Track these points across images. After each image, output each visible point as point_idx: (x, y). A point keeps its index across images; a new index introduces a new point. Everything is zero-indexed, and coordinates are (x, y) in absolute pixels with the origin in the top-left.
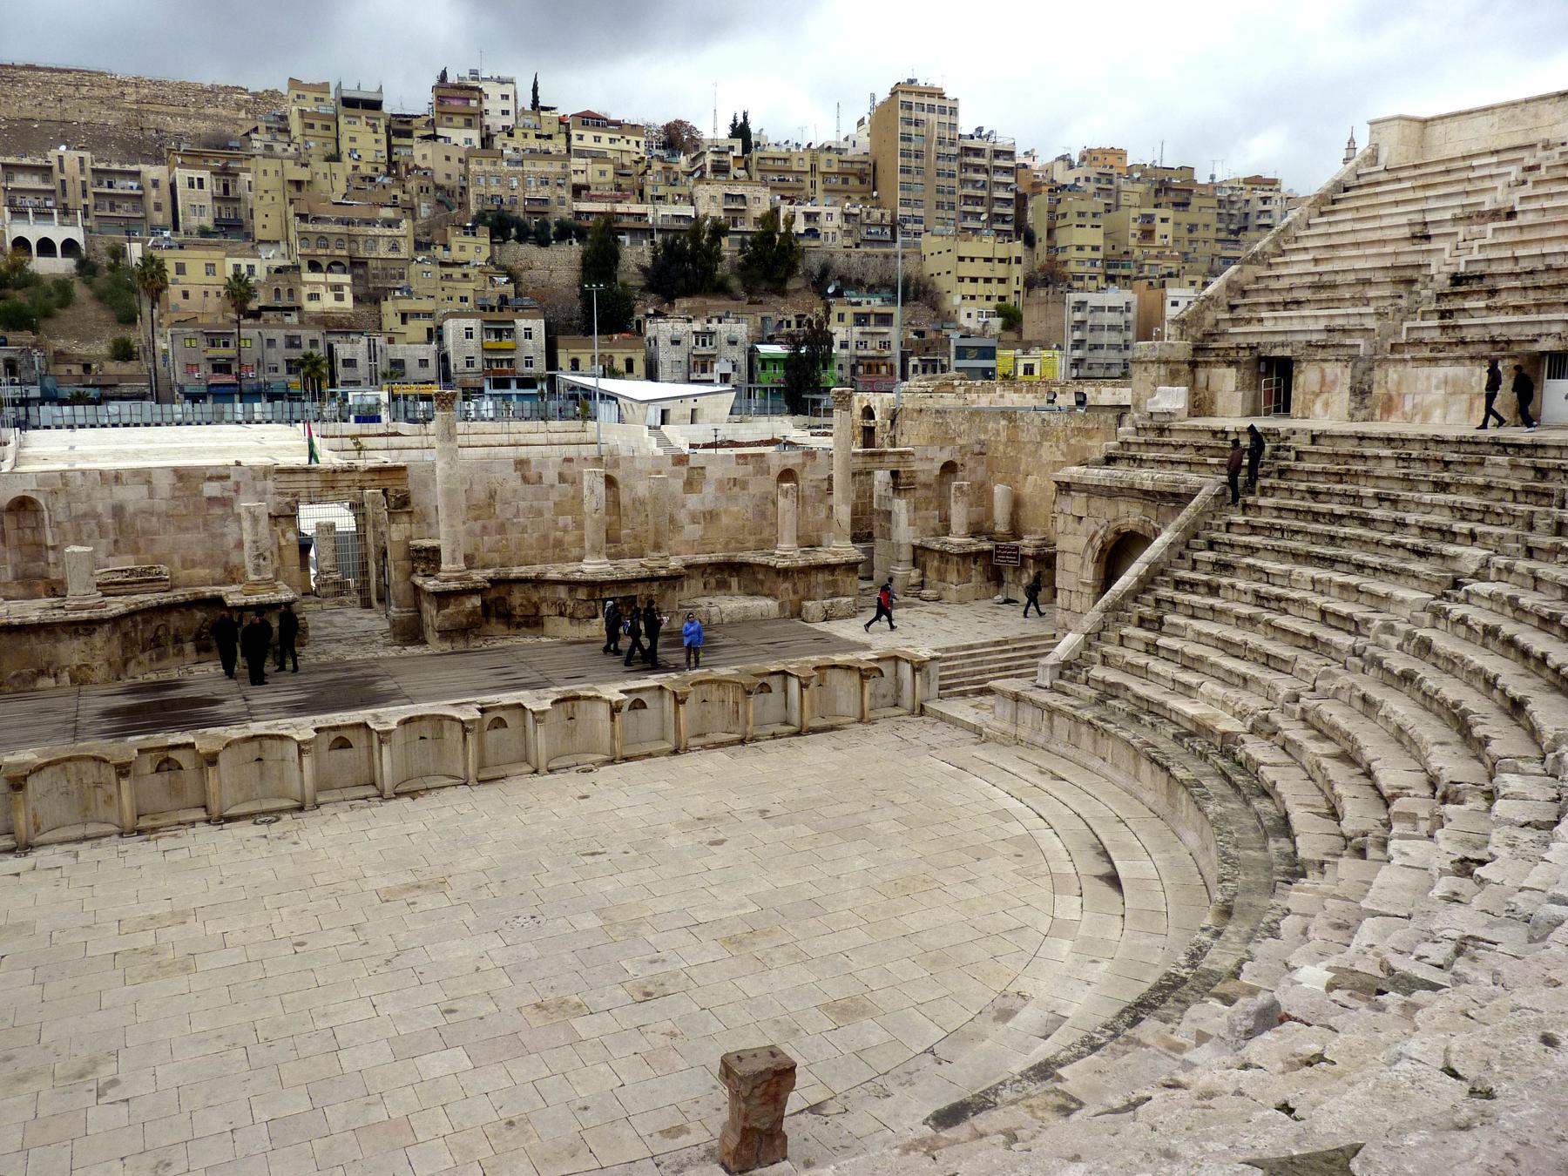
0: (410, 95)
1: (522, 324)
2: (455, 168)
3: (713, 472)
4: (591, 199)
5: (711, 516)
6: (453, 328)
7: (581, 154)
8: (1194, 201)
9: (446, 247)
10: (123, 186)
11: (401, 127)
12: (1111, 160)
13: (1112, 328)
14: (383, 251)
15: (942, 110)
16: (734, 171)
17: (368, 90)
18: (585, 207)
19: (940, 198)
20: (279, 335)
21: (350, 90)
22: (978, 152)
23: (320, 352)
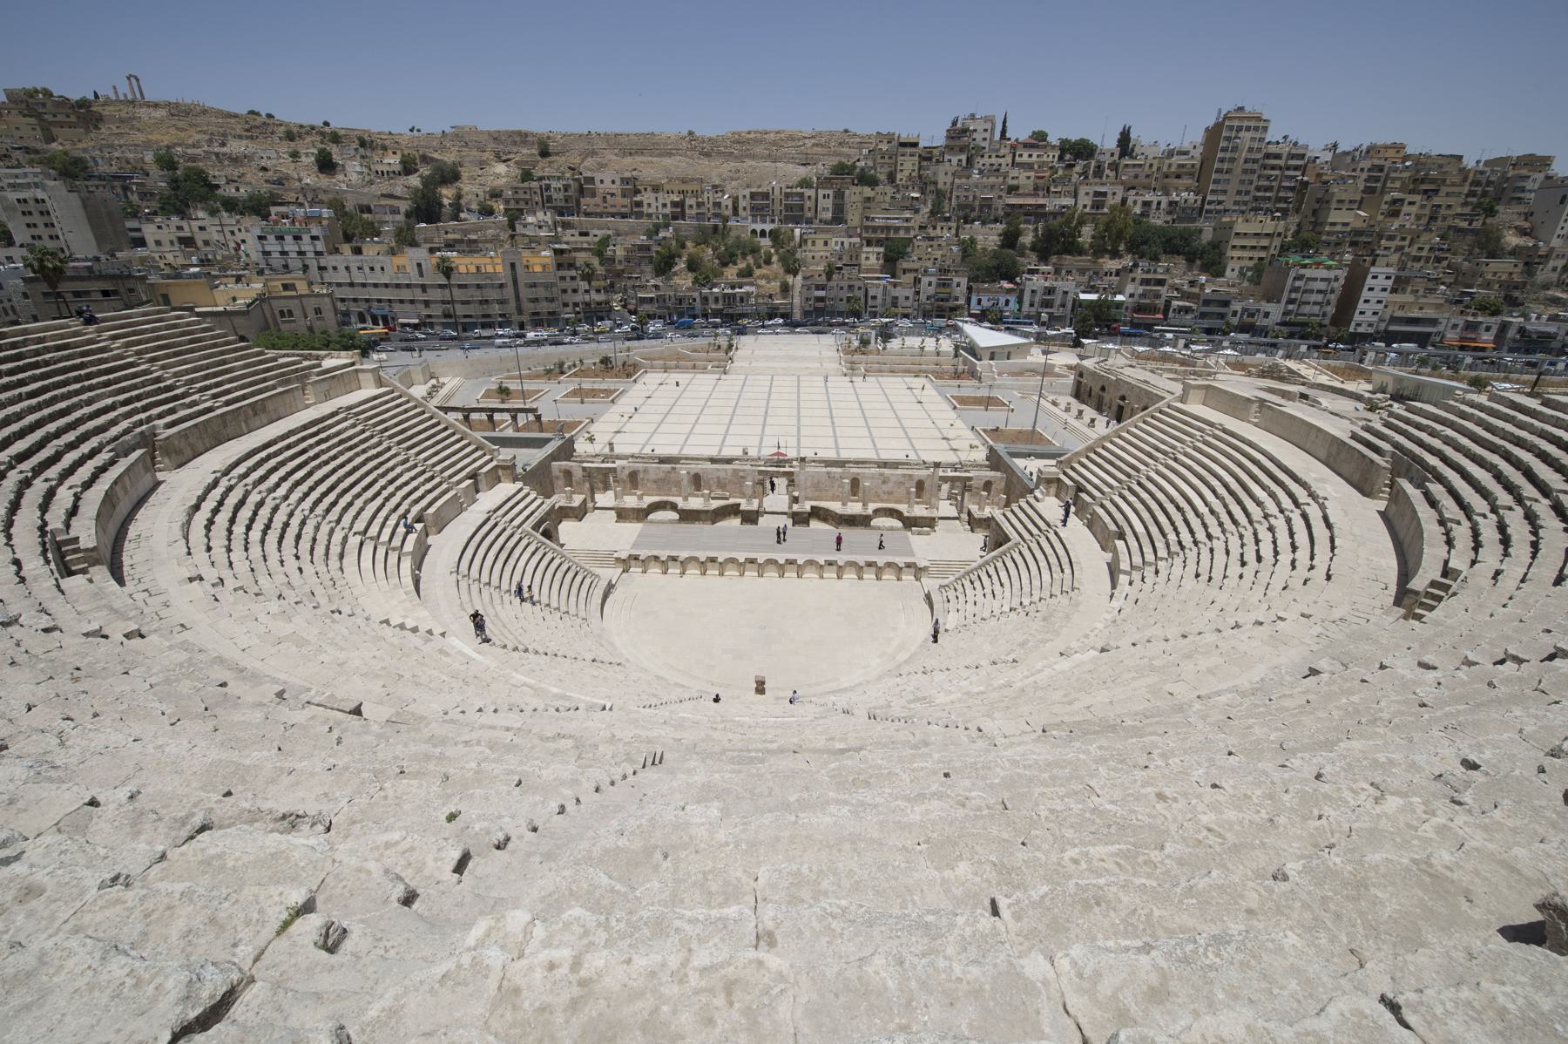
0: (933, 135)
1: (956, 280)
2: (949, 179)
3: (893, 479)
5: (890, 493)
6: (925, 280)
7: (1021, 165)
8: (1444, 190)
11: (927, 156)
12: (1391, 153)
13: (1319, 292)
14: (902, 234)
15: (1256, 129)
16: (1107, 171)
20: (845, 284)
22: (1278, 156)
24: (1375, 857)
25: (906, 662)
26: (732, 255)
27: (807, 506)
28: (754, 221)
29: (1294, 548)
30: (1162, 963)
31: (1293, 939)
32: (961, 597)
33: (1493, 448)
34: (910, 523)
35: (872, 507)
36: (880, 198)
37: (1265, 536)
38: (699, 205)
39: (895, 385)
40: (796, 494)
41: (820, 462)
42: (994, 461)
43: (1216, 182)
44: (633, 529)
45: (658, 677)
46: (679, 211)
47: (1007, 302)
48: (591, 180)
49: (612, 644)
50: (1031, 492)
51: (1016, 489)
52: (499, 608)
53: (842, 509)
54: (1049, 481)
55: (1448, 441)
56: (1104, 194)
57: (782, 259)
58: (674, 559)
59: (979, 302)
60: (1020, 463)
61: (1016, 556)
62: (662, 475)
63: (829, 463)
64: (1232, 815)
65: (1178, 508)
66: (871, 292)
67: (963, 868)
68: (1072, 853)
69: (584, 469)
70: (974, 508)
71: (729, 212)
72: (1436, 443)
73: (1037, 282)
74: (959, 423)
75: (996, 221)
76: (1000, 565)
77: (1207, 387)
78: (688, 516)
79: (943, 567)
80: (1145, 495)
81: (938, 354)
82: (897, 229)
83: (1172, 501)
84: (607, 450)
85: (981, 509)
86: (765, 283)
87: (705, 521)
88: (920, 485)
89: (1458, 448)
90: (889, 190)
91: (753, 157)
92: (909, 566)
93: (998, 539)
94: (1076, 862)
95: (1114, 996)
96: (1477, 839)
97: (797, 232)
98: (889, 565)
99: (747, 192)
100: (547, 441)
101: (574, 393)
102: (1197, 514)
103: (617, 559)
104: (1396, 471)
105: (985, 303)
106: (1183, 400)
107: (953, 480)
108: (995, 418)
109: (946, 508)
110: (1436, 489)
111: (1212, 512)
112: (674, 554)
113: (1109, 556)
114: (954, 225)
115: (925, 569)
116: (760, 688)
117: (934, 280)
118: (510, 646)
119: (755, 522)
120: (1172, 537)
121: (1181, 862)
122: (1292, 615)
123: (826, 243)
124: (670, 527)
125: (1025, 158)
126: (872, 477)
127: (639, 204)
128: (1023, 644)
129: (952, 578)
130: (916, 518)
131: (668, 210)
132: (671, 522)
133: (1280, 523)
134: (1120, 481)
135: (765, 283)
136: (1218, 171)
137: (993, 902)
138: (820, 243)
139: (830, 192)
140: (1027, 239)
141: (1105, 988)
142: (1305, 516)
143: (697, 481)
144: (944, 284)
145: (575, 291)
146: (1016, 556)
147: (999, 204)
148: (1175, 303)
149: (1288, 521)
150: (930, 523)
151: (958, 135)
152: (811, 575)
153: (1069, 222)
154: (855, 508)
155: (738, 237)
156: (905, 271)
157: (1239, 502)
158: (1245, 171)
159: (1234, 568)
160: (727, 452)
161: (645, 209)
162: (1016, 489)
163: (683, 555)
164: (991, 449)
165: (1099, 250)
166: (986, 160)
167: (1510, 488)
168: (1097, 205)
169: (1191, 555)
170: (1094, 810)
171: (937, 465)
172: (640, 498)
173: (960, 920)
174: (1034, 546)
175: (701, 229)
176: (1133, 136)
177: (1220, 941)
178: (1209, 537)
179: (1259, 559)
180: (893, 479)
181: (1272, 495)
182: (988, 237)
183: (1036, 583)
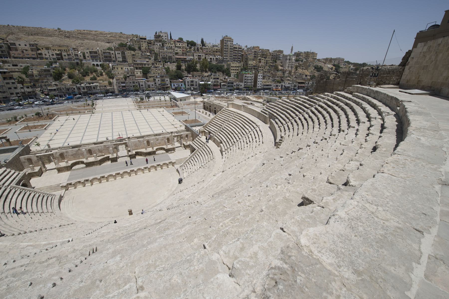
0: (151, 37)
1: (166, 79)
3: (160, 139)
4: (179, 55)
5: (160, 143)
6: (157, 79)
7: (177, 47)
9: (157, 64)
10: (108, 55)
11: (149, 42)
14: (147, 66)
17: (144, 37)
18: (177, 57)
19: (231, 55)
20: (131, 81)
21: (141, 36)
23: (137, 84)
24: (277, 200)
25: (175, 190)
26: (87, 73)
27: (134, 152)
28: (93, 61)
29: (256, 138)
30: (242, 241)
31: (265, 223)
32: (186, 168)
33: (284, 111)
34: (167, 151)
35: (155, 148)
36: (137, 55)
37: (250, 136)
38: (68, 55)
39: (154, 111)
40: (129, 149)
41: (135, 138)
42: (187, 129)
43: (225, 54)
44: (66, 174)
45: (90, 223)
46: (60, 57)
47: (182, 85)
48: (12, 44)
49: (67, 218)
50: (198, 135)
51: (194, 136)
52: (6, 221)
53: (145, 151)
54: (202, 132)
55: (277, 110)
56: (200, 56)
57: (106, 74)
58: (87, 180)
59: (174, 85)
60: (194, 128)
61: (198, 153)
62: (75, 152)
63: (138, 138)
64: (252, 201)
65: (232, 133)
66: (141, 84)
67: (196, 240)
68: (221, 224)
69: (37, 157)
70: (185, 143)
71: (82, 58)
72: (275, 111)
73: (188, 79)
74: (176, 120)
75: (174, 62)
76: (194, 157)
77: (232, 104)
78: (89, 165)
79: (180, 161)
80: (224, 132)
81: (166, 101)
82: (145, 64)
83: (230, 132)
84: (47, 147)
85: (186, 143)
86: (102, 82)
87: (97, 165)
88: (168, 139)
89: (279, 111)
90: (140, 52)
91: (88, 39)
92: (170, 163)
93: (193, 150)
94: (222, 226)
95: (234, 254)
96: (292, 189)
97: (111, 65)
98: (164, 164)
99: (88, 51)
100: (15, 149)
101: (25, 128)
102: (236, 134)
103: (62, 187)
104: (270, 118)
105: (176, 86)
106: (228, 107)
107: (177, 136)
108: (185, 117)
109: (177, 144)
110: (277, 120)
111: (239, 133)
112: (87, 179)
113: (220, 148)
114: (162, 63)
115: (175, 163)
116: (131, 213)
117: (159, 79)
118: (16, 233)
119: (116, 161)
120: (232, 140)
121: (244, 216)
122: (258, 153)
123: (122, 69)
124: (83, 170)
125: (178, 45)
126: (153, 139)
127: (41, 54)
128: (204, 176)
129: (183, 163)
130: (169, 149)
131: (55, 56)
132: (82, 168)
133: (252, 133)
134: (218, 129)
135: (102, 82)
136: (225, 51)
137: (204, 245)
138: (120, 69)
139: (120, 52)
140: (183, 67)
141: (231, 254)
142: (256, 130)
143: (90, 152)
144: (163, 81)
145: (15, 88)
146: (198, 153)
147: (174, 57)
148: (222, 84)
149: (254, 132)
150: (173, 149)
151: (158, 37)
152: (140, 173)
153: (193, 63)
154: (150, 150)
155: (88, 67)
156: (150, 77)
157: (244, 130)
158: (230, 51)
159: (246, 145)
160: (100, 140)
161: (44, 56)
162: (194, 136)
163: (91, 178)
164: (186, 126)
165: (202, 71)
166: (167, 45)
167: (288, 118)
168: (199, 59)
169: (237, 144)
170: (225, 212)
171: (172, 133)
172: (67, 162)
173: (196, 254)
174: (202, 150)
175: (71, 64)
176: (204, 41)
177: (252, 230)
178: (239, 139)
179: (250, 142)
180: (160, 139)
181: (249, 127)
182: (173, 67)
183: (204, 159)
